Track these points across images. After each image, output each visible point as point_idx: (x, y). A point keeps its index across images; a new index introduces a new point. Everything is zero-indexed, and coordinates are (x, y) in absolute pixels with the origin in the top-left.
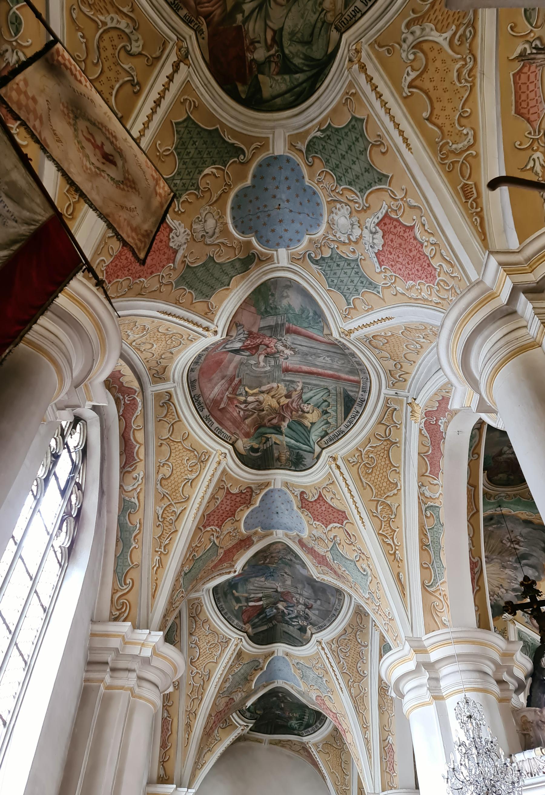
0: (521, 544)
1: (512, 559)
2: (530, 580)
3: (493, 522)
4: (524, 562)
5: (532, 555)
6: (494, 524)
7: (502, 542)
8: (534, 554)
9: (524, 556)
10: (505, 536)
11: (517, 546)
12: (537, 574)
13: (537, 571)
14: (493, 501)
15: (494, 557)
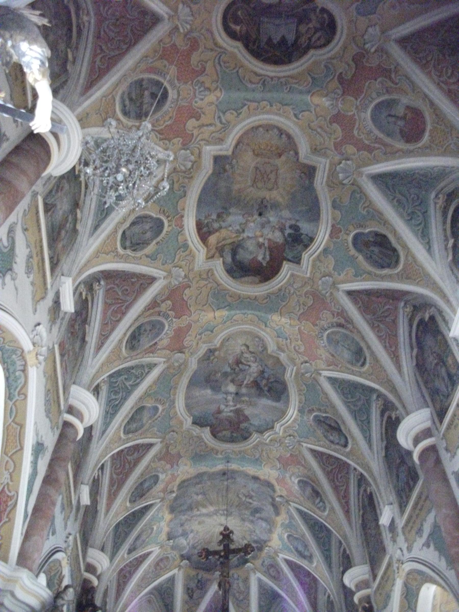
0: (254, 499)
1: (248, 512)
2: (228, 529)
3: (226, 476)
4: (258, 515)
7: (238, 496)
8: (264, 508)
11: (250, 501)
12: (268, 527)
13: (270, 525)
14: (220, 456)
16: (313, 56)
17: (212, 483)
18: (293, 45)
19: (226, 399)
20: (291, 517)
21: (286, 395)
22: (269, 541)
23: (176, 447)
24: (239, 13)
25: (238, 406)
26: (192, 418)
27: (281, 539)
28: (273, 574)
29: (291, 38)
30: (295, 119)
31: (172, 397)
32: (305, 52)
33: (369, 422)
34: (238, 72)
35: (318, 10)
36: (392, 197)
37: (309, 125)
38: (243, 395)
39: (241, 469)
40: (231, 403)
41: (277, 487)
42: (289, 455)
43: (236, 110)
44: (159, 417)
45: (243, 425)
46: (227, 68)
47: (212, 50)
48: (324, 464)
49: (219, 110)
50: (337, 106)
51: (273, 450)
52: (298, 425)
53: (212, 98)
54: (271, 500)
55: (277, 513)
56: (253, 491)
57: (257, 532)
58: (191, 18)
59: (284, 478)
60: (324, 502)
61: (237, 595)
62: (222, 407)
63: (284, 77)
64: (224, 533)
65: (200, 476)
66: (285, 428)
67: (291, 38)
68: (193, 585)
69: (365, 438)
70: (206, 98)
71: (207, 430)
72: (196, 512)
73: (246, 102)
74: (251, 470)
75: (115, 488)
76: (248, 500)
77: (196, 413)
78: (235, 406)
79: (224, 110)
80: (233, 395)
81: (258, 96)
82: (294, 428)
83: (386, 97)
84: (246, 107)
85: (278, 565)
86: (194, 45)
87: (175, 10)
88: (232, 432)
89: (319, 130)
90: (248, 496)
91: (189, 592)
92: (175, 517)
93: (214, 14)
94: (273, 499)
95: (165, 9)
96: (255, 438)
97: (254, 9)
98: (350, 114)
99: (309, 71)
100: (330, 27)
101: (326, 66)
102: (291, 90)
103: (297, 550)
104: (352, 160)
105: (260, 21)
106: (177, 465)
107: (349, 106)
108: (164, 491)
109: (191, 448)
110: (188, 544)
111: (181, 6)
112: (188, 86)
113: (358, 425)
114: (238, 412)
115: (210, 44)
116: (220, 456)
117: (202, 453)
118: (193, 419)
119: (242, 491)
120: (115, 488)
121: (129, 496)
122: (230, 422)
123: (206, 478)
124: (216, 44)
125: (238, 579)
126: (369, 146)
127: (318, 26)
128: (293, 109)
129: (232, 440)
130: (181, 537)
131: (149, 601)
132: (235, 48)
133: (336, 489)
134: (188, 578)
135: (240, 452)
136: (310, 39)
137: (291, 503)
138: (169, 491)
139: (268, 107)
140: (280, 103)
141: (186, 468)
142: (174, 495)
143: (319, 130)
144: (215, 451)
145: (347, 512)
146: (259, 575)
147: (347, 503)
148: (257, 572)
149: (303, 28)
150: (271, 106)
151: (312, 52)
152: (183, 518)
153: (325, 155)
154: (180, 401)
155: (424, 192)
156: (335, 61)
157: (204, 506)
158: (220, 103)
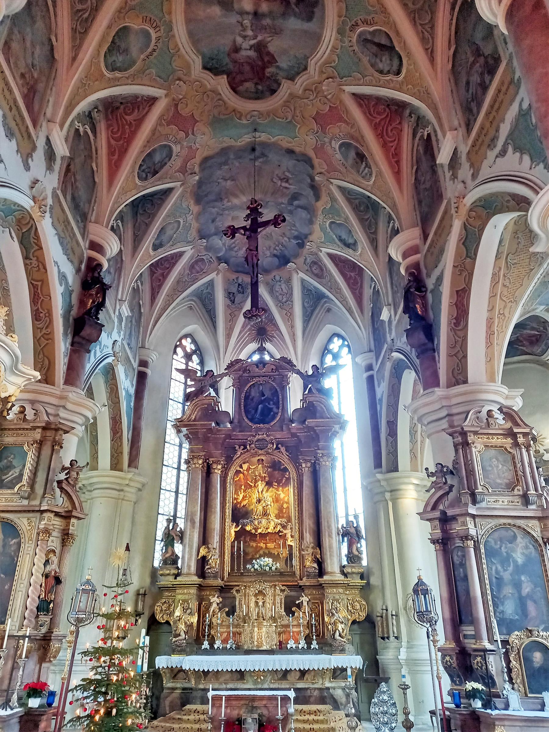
0: (291, 181)
1: (285, 200)
2: (256, 202)
4: (296, 203)
5: (302, 194)
6: (259, 157)
7: (272, 180)
9: (295, 197)
10: (273, 172)
12: (309, 216)
14: (245, 122)
15: (268, 200)
17: (240, 163)
19: (242, 25)
20: (333, 199)
21: (320, 6)
22: (310, 234)
23: (187, 105)
25: (259, 38)
26: (200, 57)
27: (323, 229)
28: (316, 272)
31: (167, 16)
33: (432, 27)
38: (264, 15)
39: (273, 140)
40: (250, 33)
41: (316, 162)
42: (328, 108)
44: (154, 50)
45: (270, 70)
48: (371, 115)
51: (308, 105)
52: (337, 55)
54: (309, 181)
55: (318, 197)
56: (289, 171)
57: (297, 225)
59: (323, 145)
60: (370, 168)
61: (280, 297)
62: (239, 40)
64: (252, 206)
65: (224, 151)
66: (321, 67)
68: (234, 289)
69: (427, 49)
71: (223, 80)
72: (226, 203)
74: (285, 142)
75: (116, 157)
76: (284, 184)
77: (205, 50)
78: (255, 37)
80: (250, 17)
82: (333, 65)
85: (321, 260)
88: (256, 84)
90: (284, 178)
91: (230, 296)
92: (204, 209)
94: (312, 179)
96: (286, 89)
103: (341, 240)
106: (193, 134)
108: (183, 170)
109: (207, 108)
110: (224, 244)
113: (417, 33)
114: (260, 48)
116: (245, 122)
117: (222, 117)
118: (203, 58)
119: (276, 172)
120: (116, 157)
121: (137, 170)
122: (252, 68)
123: (232, 156)
125: (280, 281)
129: (258, 96)
130: (214, 237)
131: (191, 308)
133: (385, 146)
134: (227, 282)
135: (268, 114)
137: (332, 180)
138: (189, 172)
141: (205, 138)
142: (197, 178)
144: (238, 116)
145: (397, 174)
146: (301, 275)
147: (398, 162)
148: (299, 271)
152: (214, 210)
154: (179, 23)
157: (236, 196)
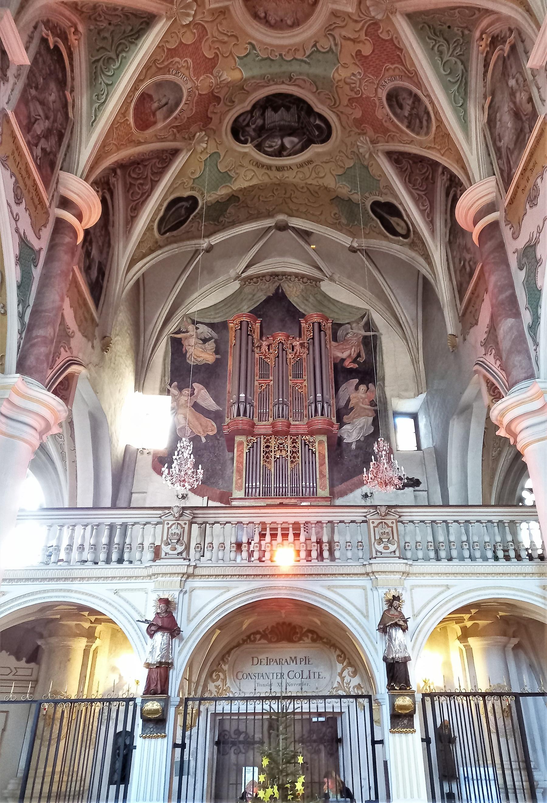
16: (247, 106)
18: (267, 108)
24: (317, 133)
29: (269, 113)
30: (254, 42)
32: (254, 107)
34: (317, 90)
35: (250, 140)
36: (126, 9)
37: (238, 41)
43: (318, 51)
46: (328, 94)
47: (342, 112)
49: (336, 55)
50: (215, 77)
53: (344, 74)
58: (358, 143)
63: (271, 85)
67: (269, 113)
70: (349, 75)
73: (307, 59)
79: (330, 53)
81: (295, 68)
83: (175, 114)
84: (308, 53)
86: (359, 123)
87: (371, 155)
89: (226, 39)
93: (338, 140)
95: (378, 160)
97: (304, 134)
98: (201, 78)
99: (248, 93)
100: (238, 132)
101: (234, 102)
102: (263, 77)
104: (184, 26)
105: (298, 122)
107: (205, 83)
111: (367, 156)
112: (366, 94)
115: (343, 117)
124: (338, 115)
126: (172, 57)
127: (247, 129)
128: (257, 56)
132: (319, 108)
136: (252, 117)
139: (284, 53)
140: (272, 60)
143: (226, 39)
149: (260, 122)
150: (281, 55)
151: (249, 108)
153: (213, 12)
155: (92, 27)
156: (227, 109)
158: (335, 65)
